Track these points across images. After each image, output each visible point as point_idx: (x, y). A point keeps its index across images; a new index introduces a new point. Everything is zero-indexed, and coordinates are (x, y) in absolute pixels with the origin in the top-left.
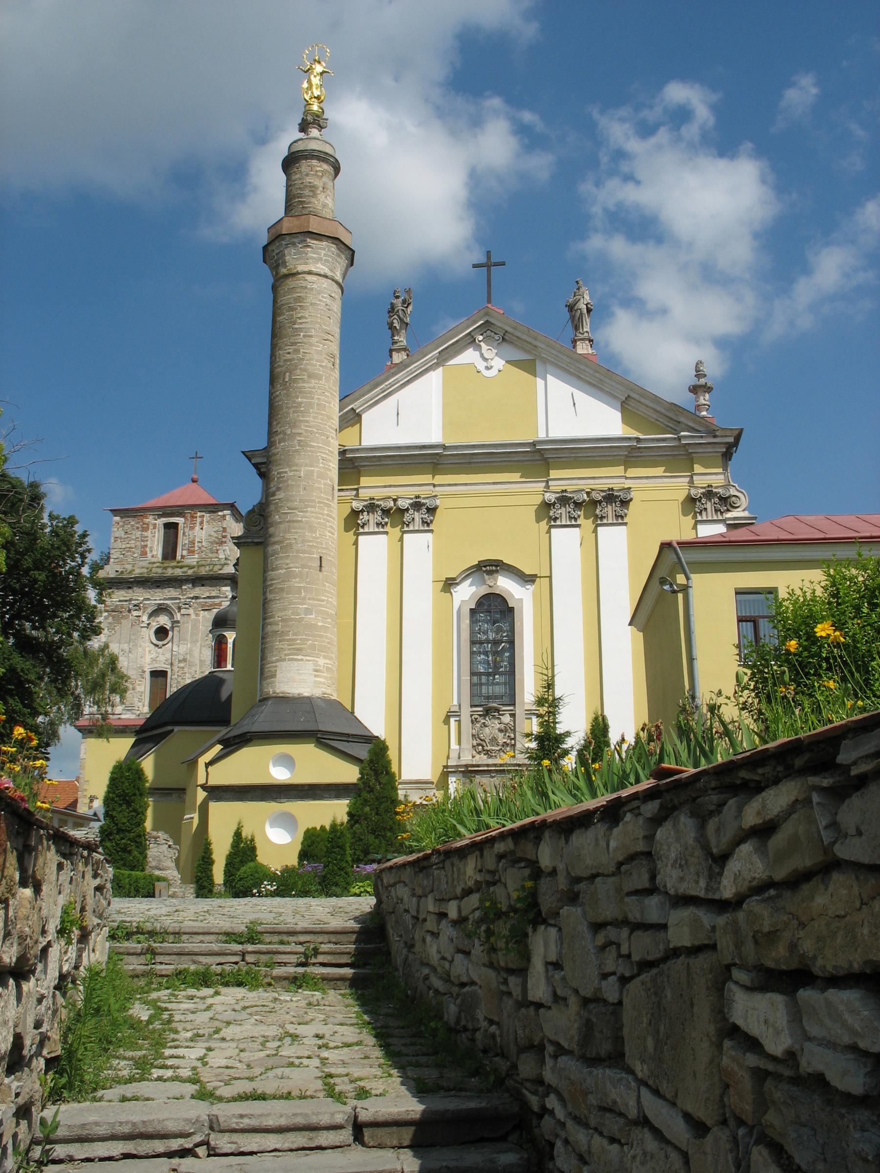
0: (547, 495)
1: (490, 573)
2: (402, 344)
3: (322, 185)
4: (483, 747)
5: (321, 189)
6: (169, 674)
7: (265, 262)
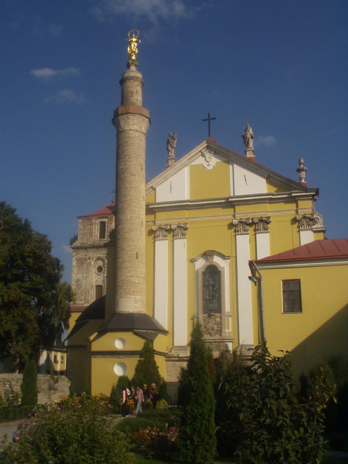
0: (234, 221)
1: (210, 255)
2: (172, 157)
3: (135, 91)
4: (208, 331)
5: (135, 93)
6: (103, 287)
7: (114, 125)
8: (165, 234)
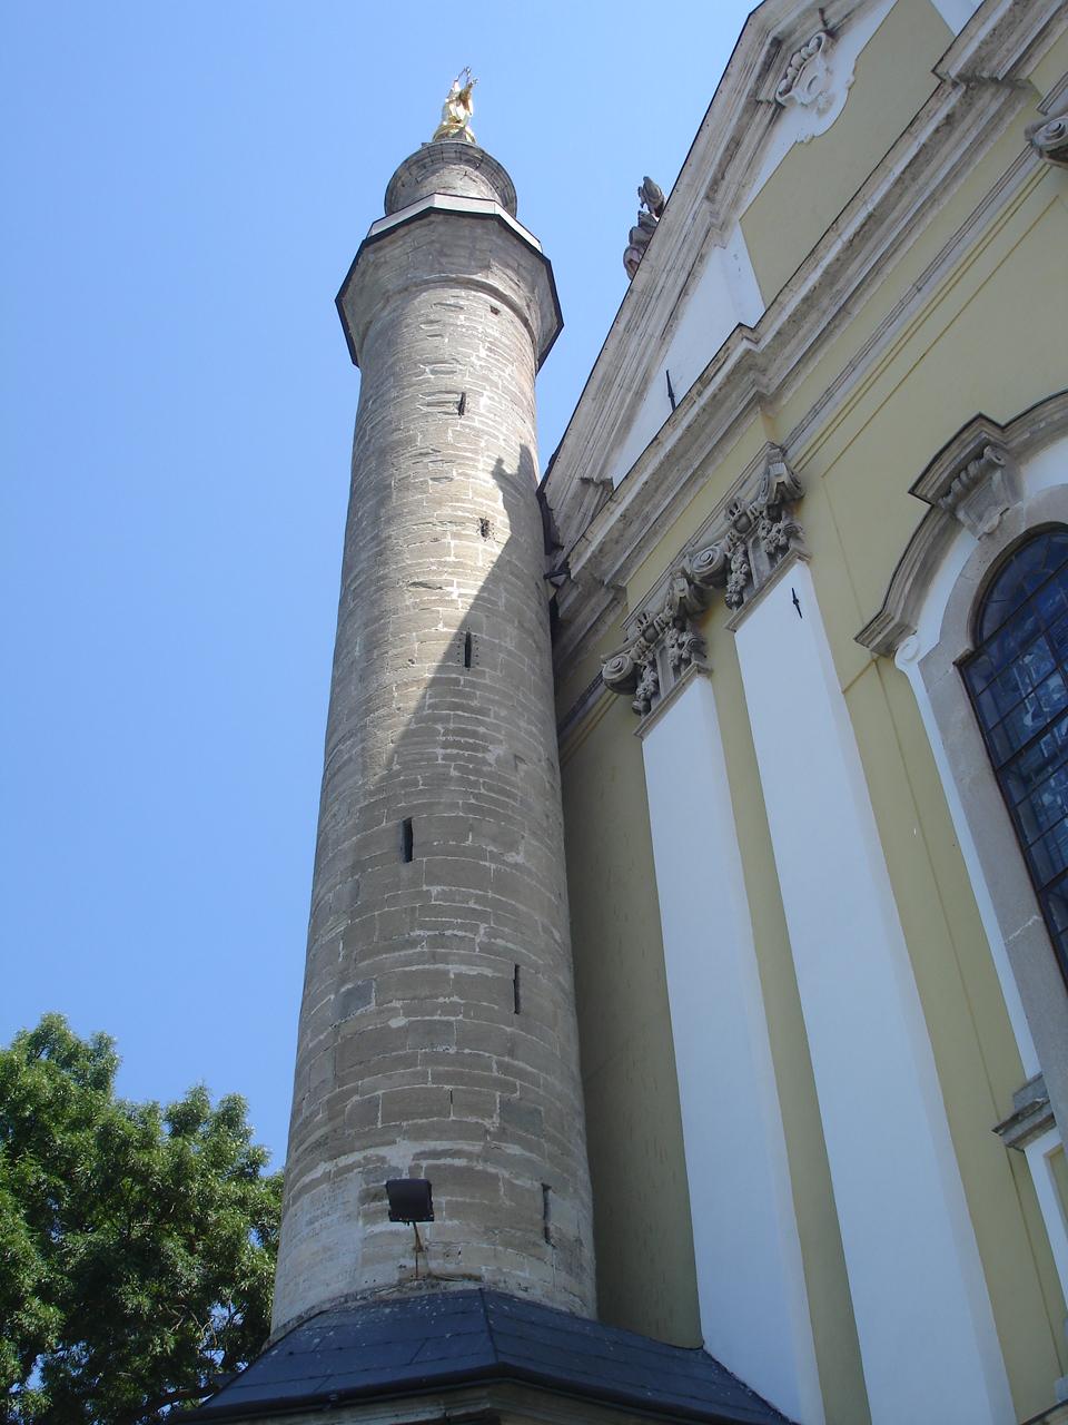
8: (681, 646)
